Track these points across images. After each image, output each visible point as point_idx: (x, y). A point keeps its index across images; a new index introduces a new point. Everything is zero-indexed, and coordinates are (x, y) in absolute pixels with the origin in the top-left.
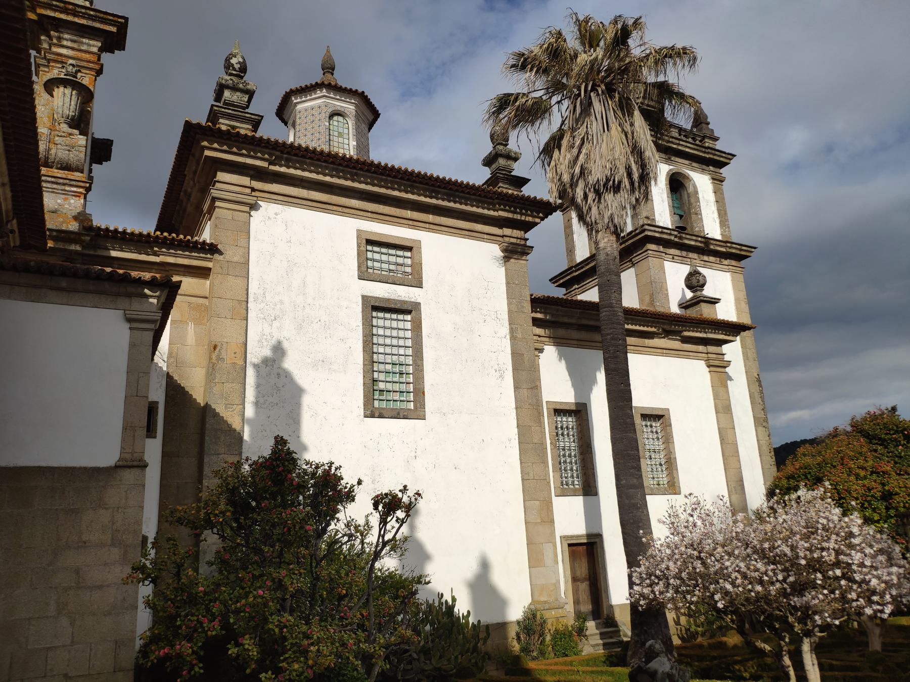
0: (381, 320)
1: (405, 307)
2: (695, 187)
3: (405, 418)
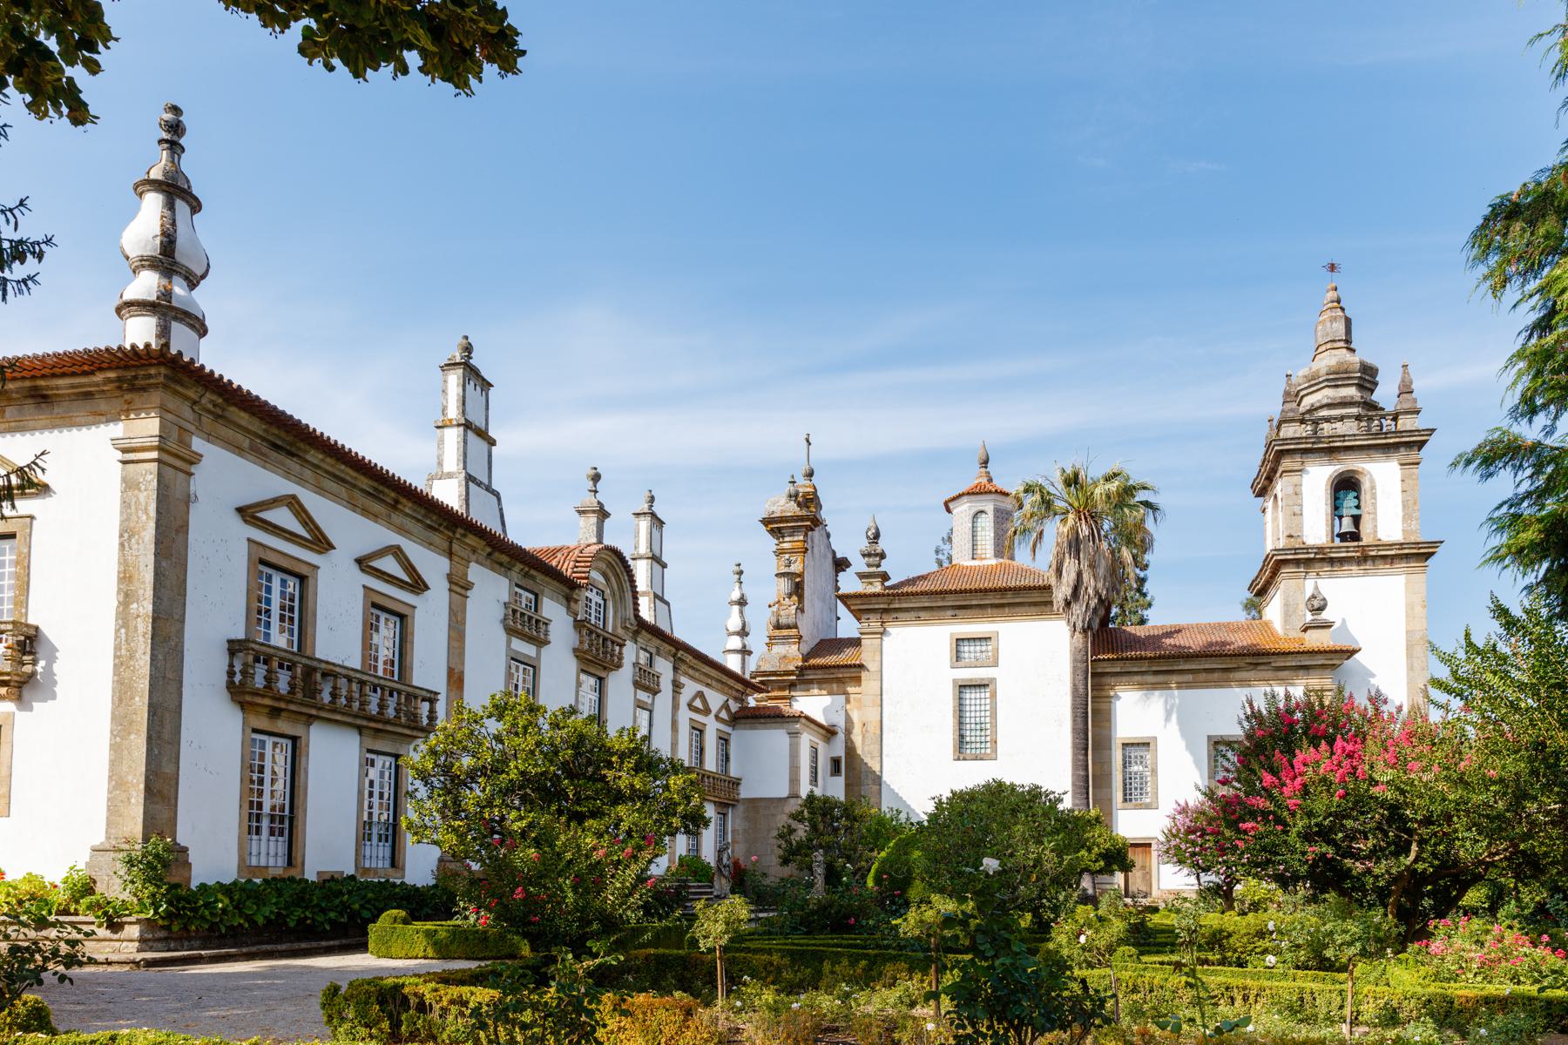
0: (969, 695)
1: (983, 683)
2: (1372, 481)
3: (981, 759)
